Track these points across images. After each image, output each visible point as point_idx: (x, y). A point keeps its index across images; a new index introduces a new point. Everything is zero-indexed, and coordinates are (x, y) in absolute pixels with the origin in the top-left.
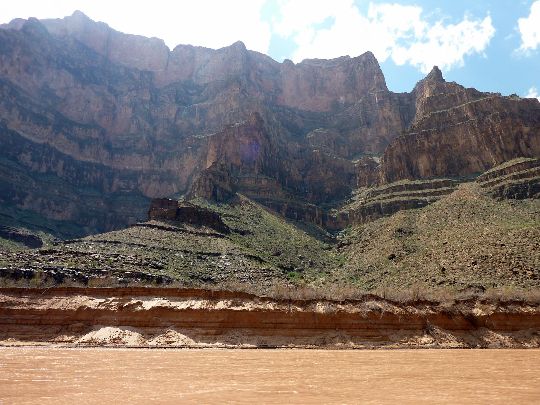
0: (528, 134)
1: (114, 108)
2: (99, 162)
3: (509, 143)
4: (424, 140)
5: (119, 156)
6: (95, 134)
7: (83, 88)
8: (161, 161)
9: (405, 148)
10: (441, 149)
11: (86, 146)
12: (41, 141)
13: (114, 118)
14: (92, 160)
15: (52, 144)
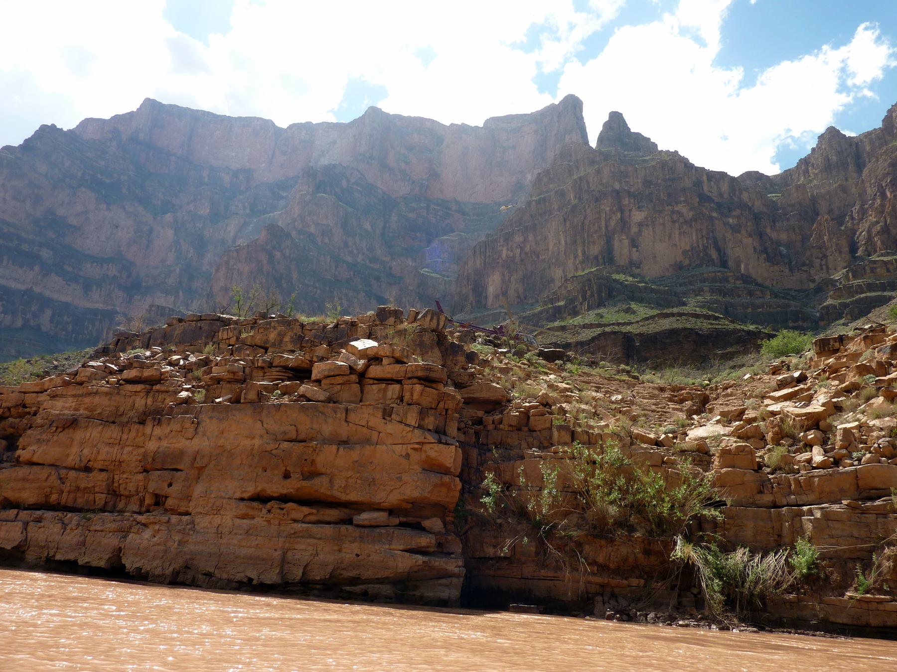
0: (640, 225)
1: (151, 231)
2: (110, 308)
3: (594, 243)
4: (502, 246)
5: (139, 297)
6: (113, 271)
7: (108, 209)
8: (190, 301)
9: (478, 262)
10: (522, 260)
11: (94, 288)
12: (23, 287)
13: (148, 246)
14: (101, 306)
15: (37, 290)
